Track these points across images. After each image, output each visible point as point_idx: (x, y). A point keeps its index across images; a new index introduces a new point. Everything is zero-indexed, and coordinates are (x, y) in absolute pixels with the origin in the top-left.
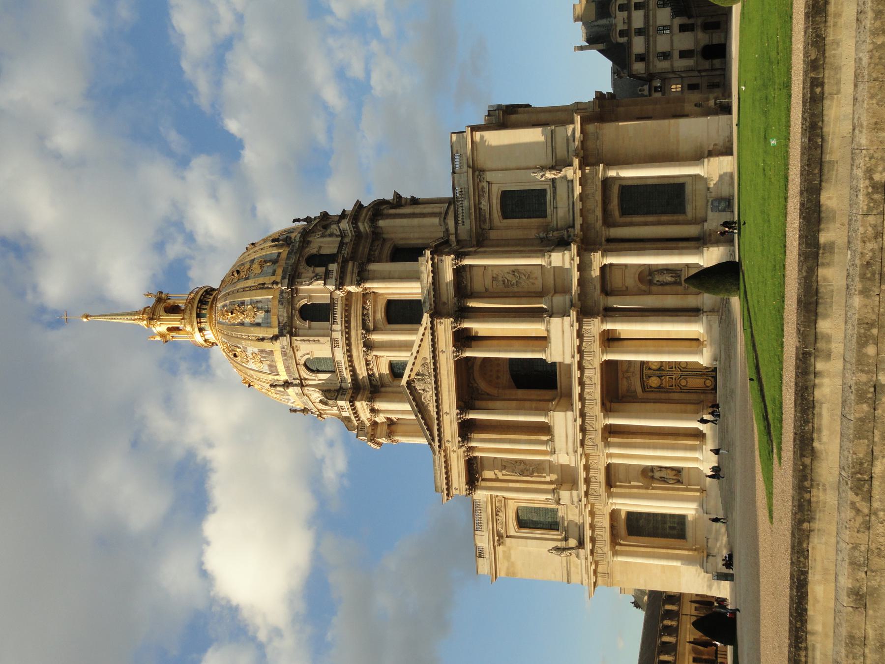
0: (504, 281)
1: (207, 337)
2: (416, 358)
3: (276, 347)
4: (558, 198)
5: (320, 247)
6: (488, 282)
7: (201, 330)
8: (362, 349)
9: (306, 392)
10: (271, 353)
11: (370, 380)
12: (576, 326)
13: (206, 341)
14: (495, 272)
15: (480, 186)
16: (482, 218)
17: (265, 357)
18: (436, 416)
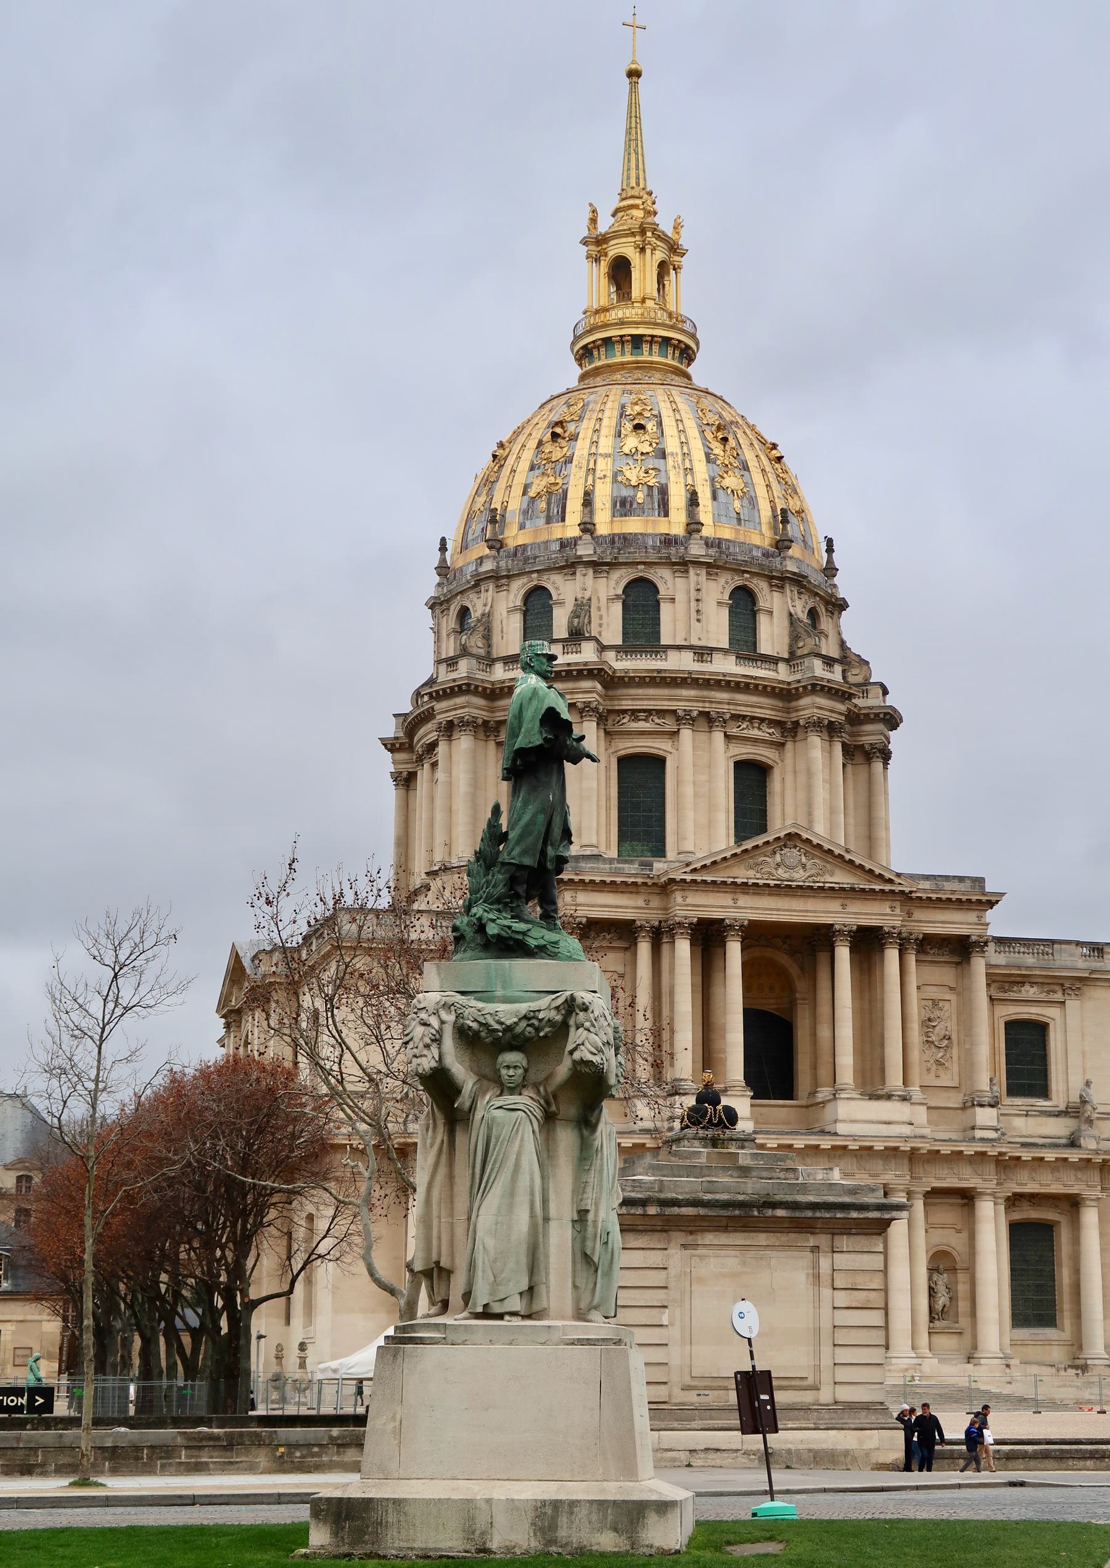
0: (929, 1020)
1: (618, 347)
2: (841, 857)
3: (676, 523)
4: (1043, 1119)
5: (827, 636)
6: (932, 993)
7: (637, 341)
8: (696, 708)
9: (580, 570)
10: (664, 509)
11: (625, 712)
12: (906, 1147)
13: (607, 341)
14: (947, 1005)
15: (1057, 988)
16: (1007, 986)
17: (650, 495)
18: (739, 881)
